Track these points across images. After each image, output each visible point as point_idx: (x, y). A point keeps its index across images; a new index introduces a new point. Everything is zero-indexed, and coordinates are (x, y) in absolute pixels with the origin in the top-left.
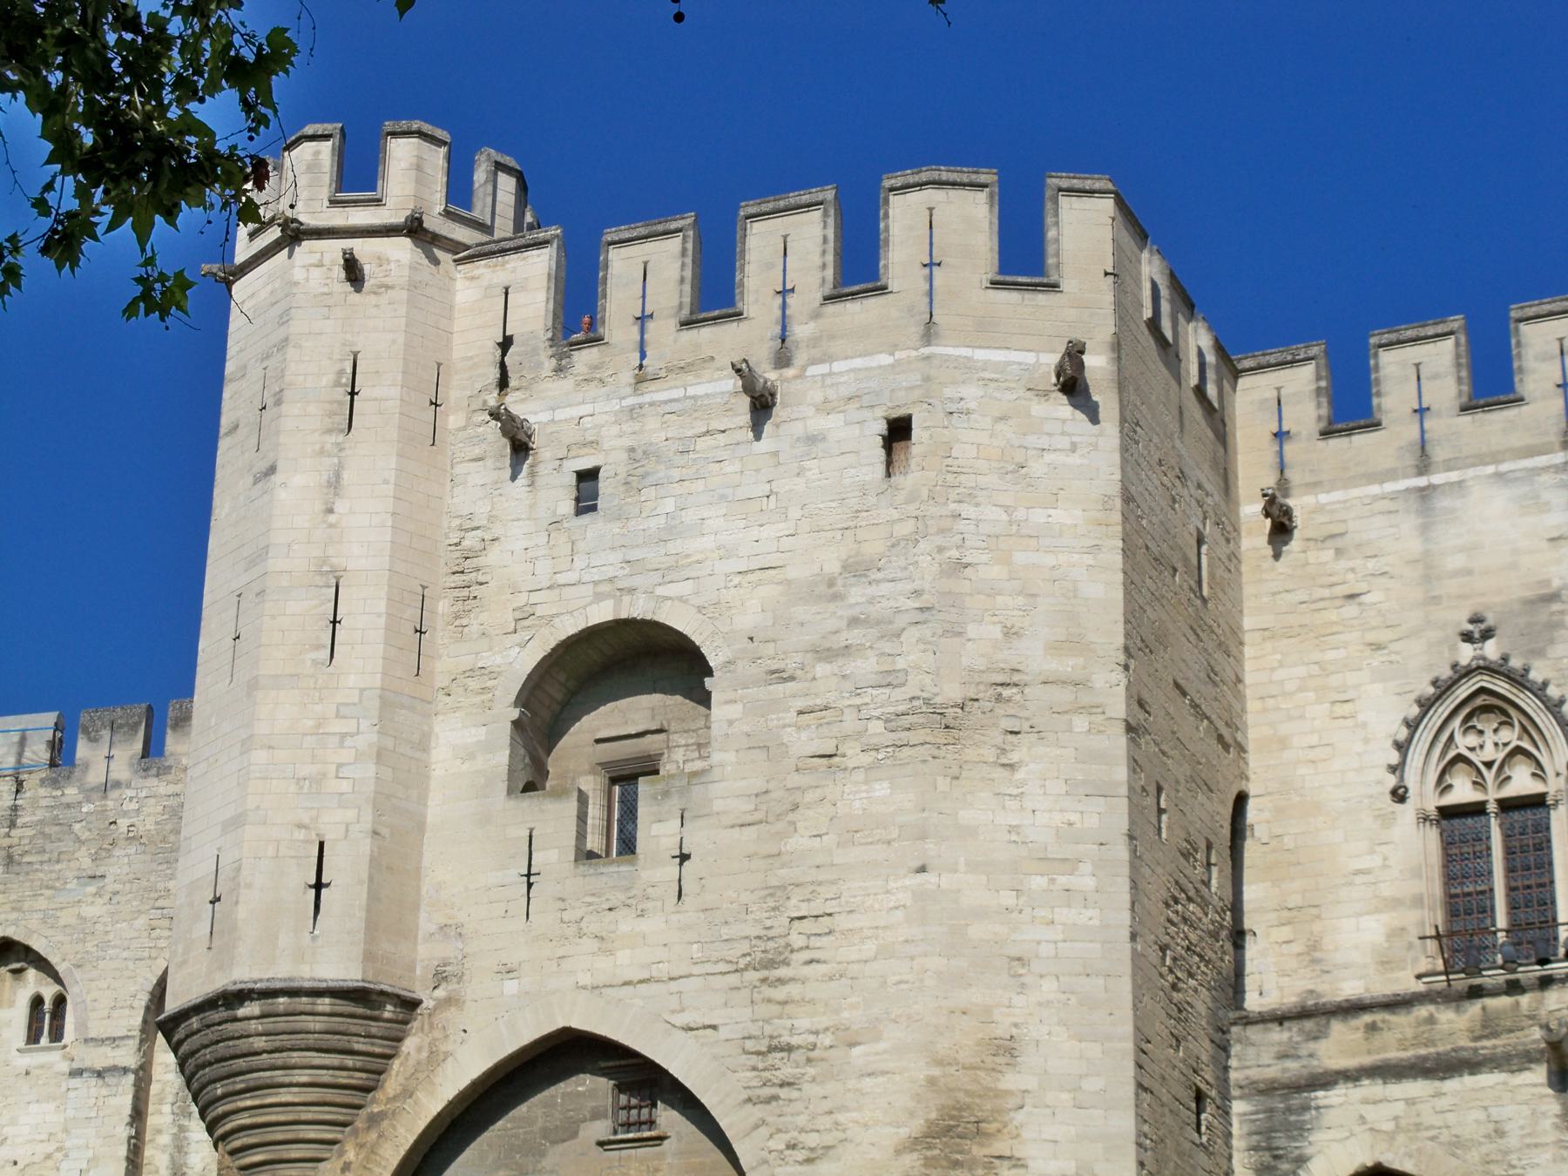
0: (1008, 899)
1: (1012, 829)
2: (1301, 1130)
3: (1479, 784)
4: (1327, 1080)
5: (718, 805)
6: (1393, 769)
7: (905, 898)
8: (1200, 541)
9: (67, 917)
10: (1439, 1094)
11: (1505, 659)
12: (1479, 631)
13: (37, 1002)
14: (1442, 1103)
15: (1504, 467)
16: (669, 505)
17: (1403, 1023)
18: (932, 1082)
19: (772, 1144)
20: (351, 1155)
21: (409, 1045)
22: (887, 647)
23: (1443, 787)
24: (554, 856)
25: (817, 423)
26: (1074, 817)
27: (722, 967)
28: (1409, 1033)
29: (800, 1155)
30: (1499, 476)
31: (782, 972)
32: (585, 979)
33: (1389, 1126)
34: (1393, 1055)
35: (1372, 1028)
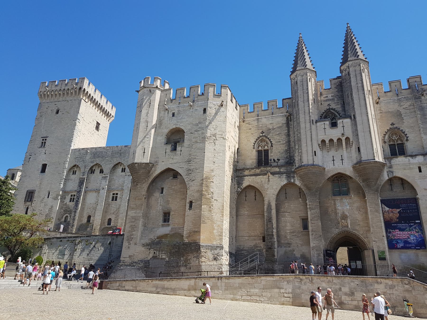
2: (243, 181)
3: (262, 148)
5: (185, 146)
6: (253, 146)
7: (203, 155)
8: (235, 122)
9: (126, 160)
11: (265, 135)
12: (263, 133)
13: (123, 168)
14: (256, 179)
15: (266, 117)
17: (253, 171)
18: (205, 174)
19: (188, 179)
20: (146, 180)
21: (153, 169)
23: (258, 148)
25: (197, 108)
27: (184, 162)
28: (253, 171)
29: (191, 181)
31: (190, 162)
35: (250, 171)
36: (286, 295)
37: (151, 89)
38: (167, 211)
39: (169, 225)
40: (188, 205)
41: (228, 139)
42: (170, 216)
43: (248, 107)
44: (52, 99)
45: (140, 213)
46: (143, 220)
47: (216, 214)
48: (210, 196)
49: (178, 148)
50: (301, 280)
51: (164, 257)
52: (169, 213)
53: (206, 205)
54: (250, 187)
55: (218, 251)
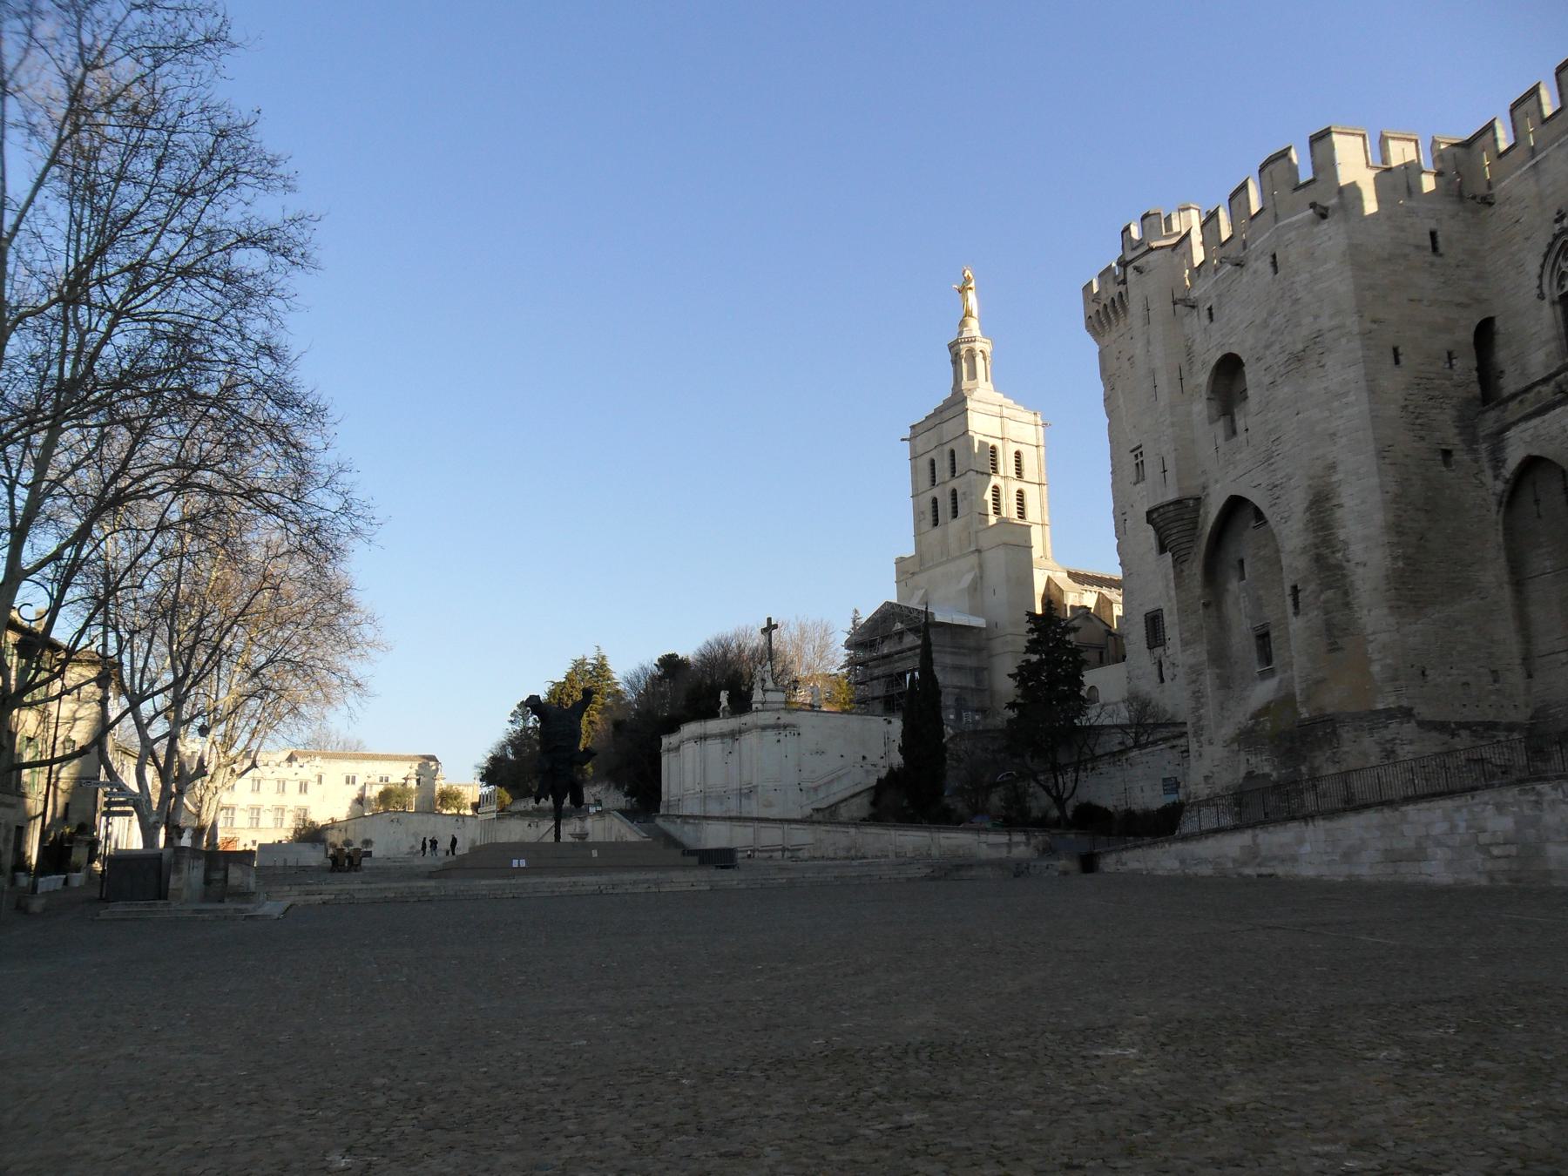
0: (1327, 414)
1: (1326, 388)
2: (1502, 449)
4: (1507, 428)
8: (1433, 235)
10: (1544, 422)
14: (1546, 424)
15: (1561, 141)
16: (1227, 311)
17: (1531, 395)
18: (1310, 486)
20: (1195, 550)
21: (1201, 512)
22: (1280, 338)
23: (1563, 286)
24: (1220, 441)
26: (1345, 376)
30: (1559, 146)
31: (1273, 460)
32: (1232, 478)
33: (1529, 439)
34: (1530, 410)
35: (1521, 402)
36: (1496, 851)
37: (1136, 264)
38: (1263, 631)
39: (1272, 673)
40: (1289, 601)
41: (1375, 326)
42: (1272, 645)
43: (1494, 133)
44: (1121, 324)
45: (1200, 653)
46: (1218, 671)
47: (1369, 611)
48: (1339, 555)
49: (1240, 424)
50: (1539, 794)
51: (1267, 770)
52: (1267, 635)
53: (1331, 588)
54: (1531, 464)
55: (1394, 725)
